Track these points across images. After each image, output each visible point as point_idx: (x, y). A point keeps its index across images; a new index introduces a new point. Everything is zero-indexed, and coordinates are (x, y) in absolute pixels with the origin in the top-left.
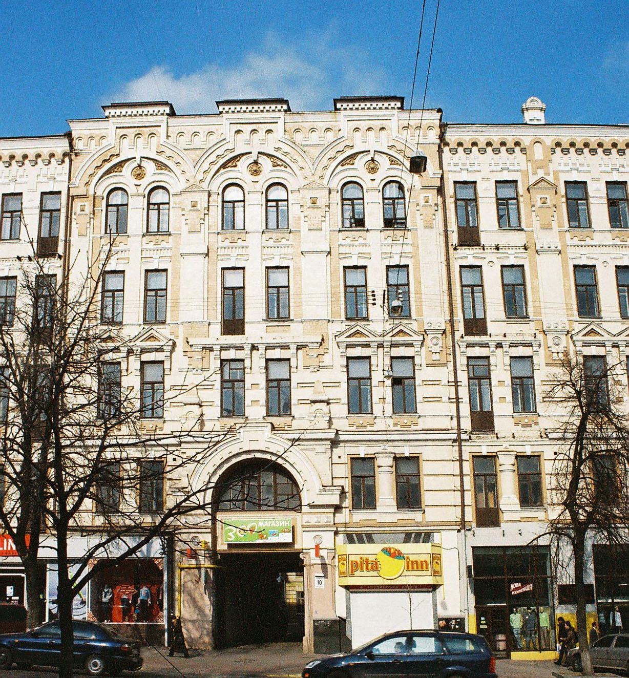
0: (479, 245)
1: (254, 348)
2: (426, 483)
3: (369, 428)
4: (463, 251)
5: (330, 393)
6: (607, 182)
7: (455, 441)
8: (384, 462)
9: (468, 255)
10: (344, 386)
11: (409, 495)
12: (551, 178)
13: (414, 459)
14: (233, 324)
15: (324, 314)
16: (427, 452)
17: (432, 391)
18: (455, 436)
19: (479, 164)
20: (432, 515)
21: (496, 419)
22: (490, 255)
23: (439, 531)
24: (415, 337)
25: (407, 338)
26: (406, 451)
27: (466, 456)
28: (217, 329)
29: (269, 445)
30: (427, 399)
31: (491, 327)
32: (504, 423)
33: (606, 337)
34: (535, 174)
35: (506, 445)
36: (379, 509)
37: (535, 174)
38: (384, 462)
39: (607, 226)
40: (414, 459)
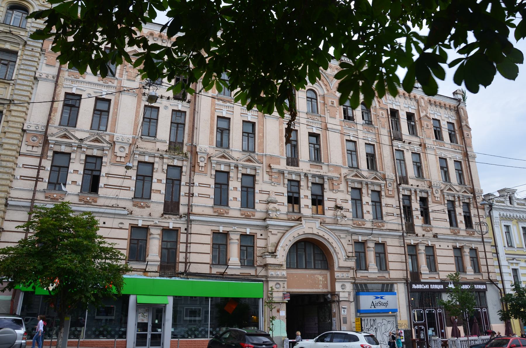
0: (402, 140)
1: (306, 175)
2: (390, 257)
3: (363, 226)
4: (395, 143)
5: (344, 205)
6: (448, 122)
7: (400, 236)
8: (371, 245)
9: (398, 144)
10: (350, 202)
11: (382, 263)
12: (428, 115)
13: (383, 244)
14: (293, 161)
15: (340, 162)
16: (389, 241)
17: (390, 210)
18: (401, 234)
19: (399, 102)
20: (393, 275)
21: (415, 227)
22: (407, 146)
23: (396, 283)
24: (381, 182)
25: (377, 181)
26: (380, 240)
27: (406, 246)
28: (284, 162)
29: (319, 231)
30: (388, 214)
31: (411, 181)
32: (418, 230)
33: (455, 192)
34: (422, 112)
35: (420, 240)
36: (370, 271)
37: (422, 112)
38: (371, 245)
39: (449, 142)
40: (383, 244)
